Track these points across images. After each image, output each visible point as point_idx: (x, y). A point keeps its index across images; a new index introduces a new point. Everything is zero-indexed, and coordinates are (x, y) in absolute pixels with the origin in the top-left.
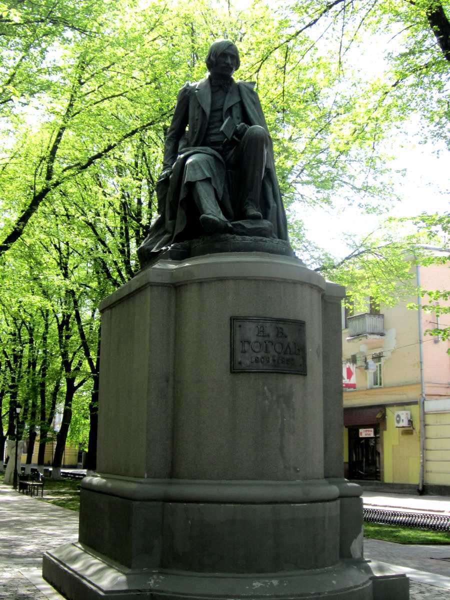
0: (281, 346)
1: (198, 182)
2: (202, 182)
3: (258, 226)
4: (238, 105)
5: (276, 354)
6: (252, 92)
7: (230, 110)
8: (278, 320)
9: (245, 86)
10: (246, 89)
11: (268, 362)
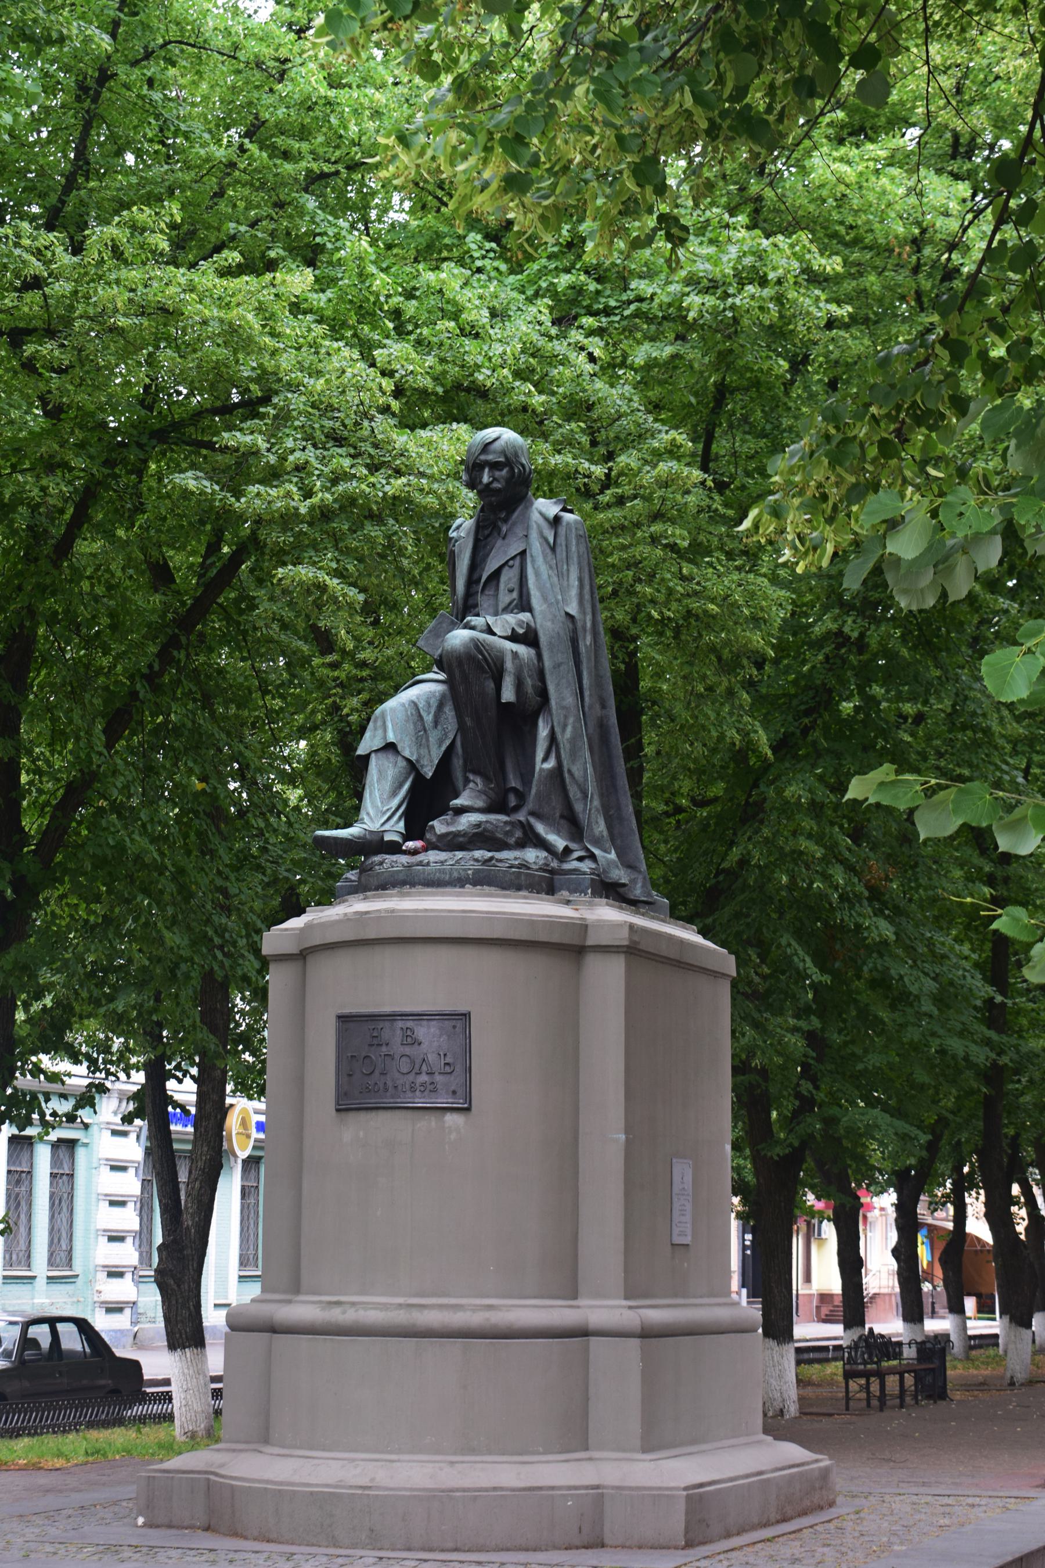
2: (379, 754)
5: (397, 1075)
7: (496, 574)
9: (541, 514)
10: (541, 521)
11: (386, 1090)
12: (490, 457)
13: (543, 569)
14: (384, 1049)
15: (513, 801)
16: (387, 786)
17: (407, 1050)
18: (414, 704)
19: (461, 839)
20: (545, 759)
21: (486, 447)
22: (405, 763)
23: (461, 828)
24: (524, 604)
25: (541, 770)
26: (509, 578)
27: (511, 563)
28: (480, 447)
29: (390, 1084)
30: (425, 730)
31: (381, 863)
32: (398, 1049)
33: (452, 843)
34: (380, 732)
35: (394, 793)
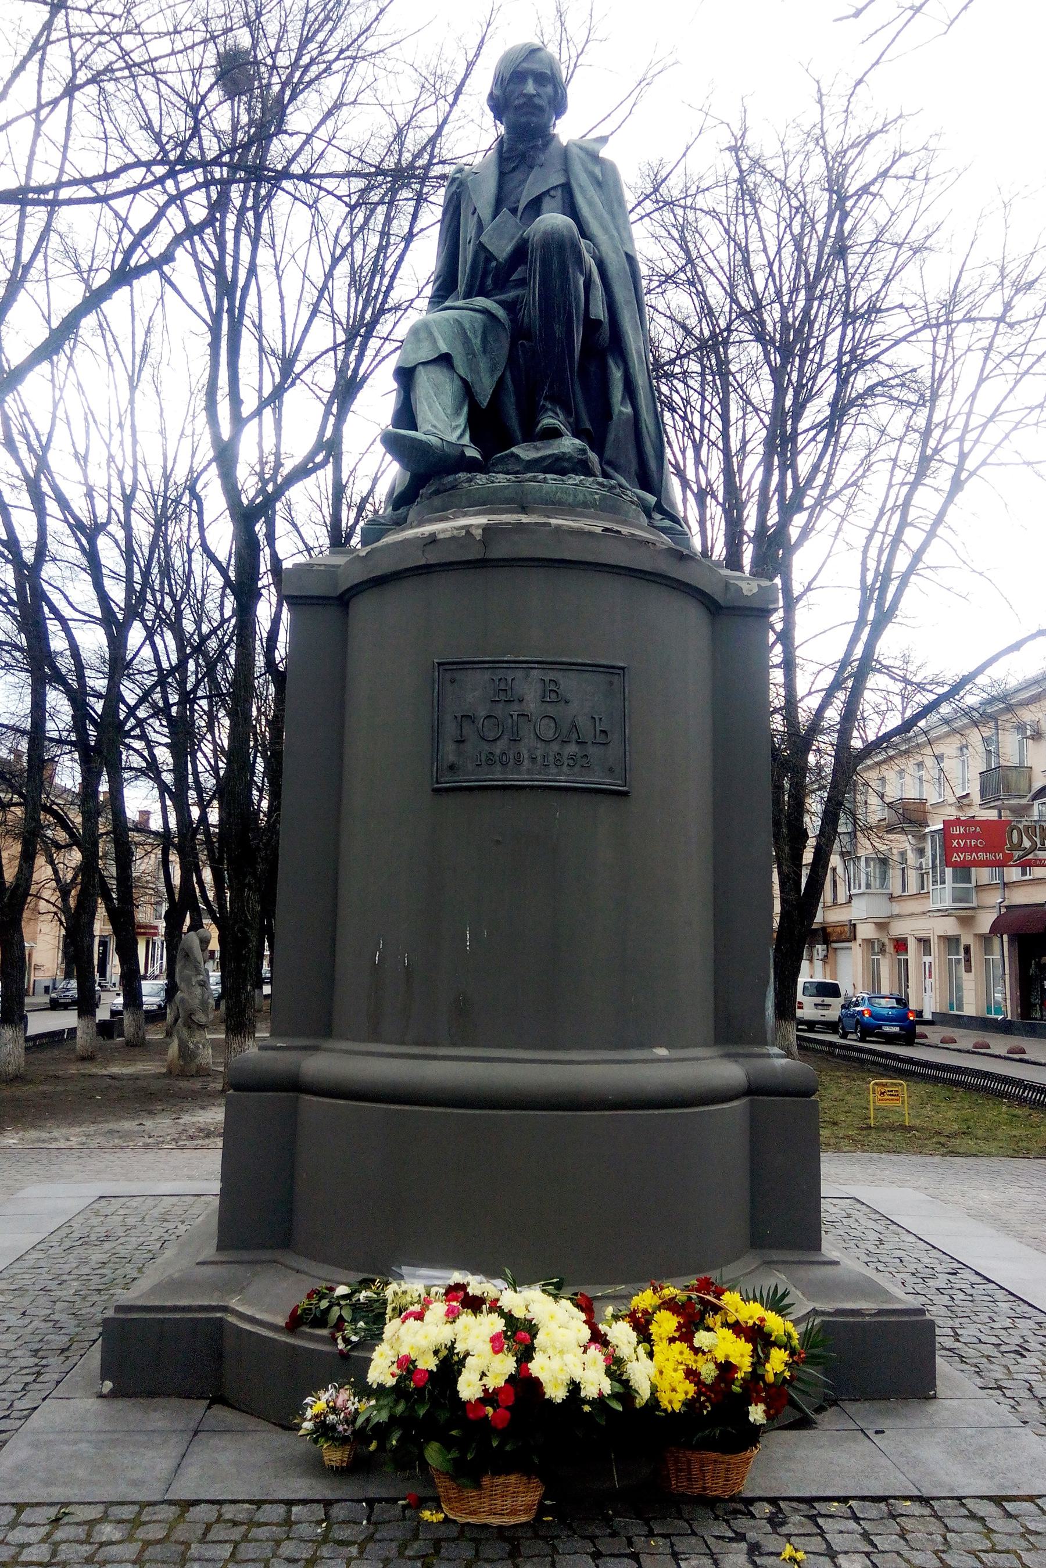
0: (553, 725)
1: (420, 368)
2: (430, 368)
3: (549, 452)
4: (558, 193)
6: (595, 158)
9: (581, 148)
10: (582, 155)
11: (519, 762)
12: (535, 66)
13: (597, 199)
14: (516, 706)
17: (550, 710)
19: (565, 464)
20: (622, 403)
22: (458, 382)
23: (565, 450)
25: (621, 412)
27: (552, 193)
28: (524, 53)
29: (525, 754)
30: (474, 355)
31: (470, 480)
32: (532, 704)
35: (457, 412)
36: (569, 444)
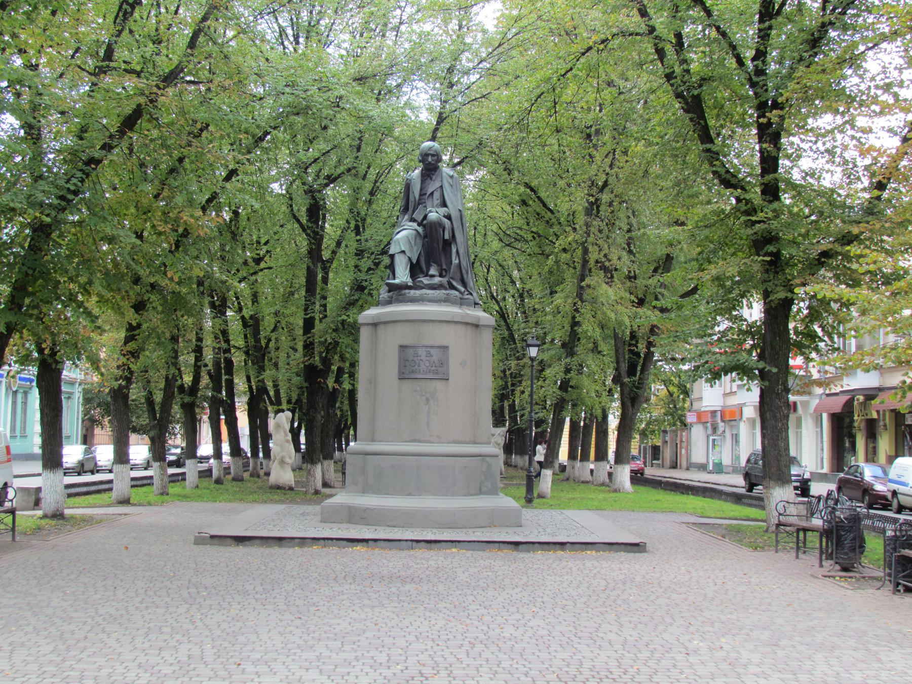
7: (432, 193)
8: (427, 347)
15: (444, 273)
16: (404, 265)
18: (408, 237)
21: (430, 148)
24: (444, 204)
26: (437, 195)
32: (423, 358)
33: (432, 287)
34: (398, 247)
36: (437, 280)
